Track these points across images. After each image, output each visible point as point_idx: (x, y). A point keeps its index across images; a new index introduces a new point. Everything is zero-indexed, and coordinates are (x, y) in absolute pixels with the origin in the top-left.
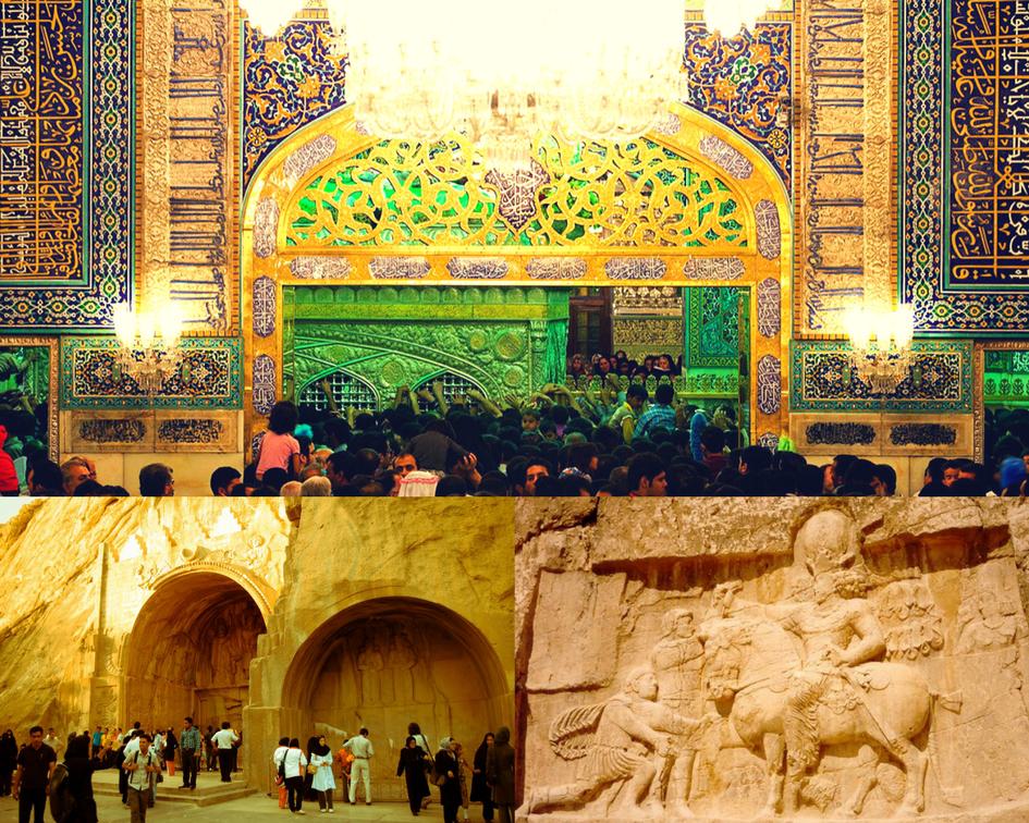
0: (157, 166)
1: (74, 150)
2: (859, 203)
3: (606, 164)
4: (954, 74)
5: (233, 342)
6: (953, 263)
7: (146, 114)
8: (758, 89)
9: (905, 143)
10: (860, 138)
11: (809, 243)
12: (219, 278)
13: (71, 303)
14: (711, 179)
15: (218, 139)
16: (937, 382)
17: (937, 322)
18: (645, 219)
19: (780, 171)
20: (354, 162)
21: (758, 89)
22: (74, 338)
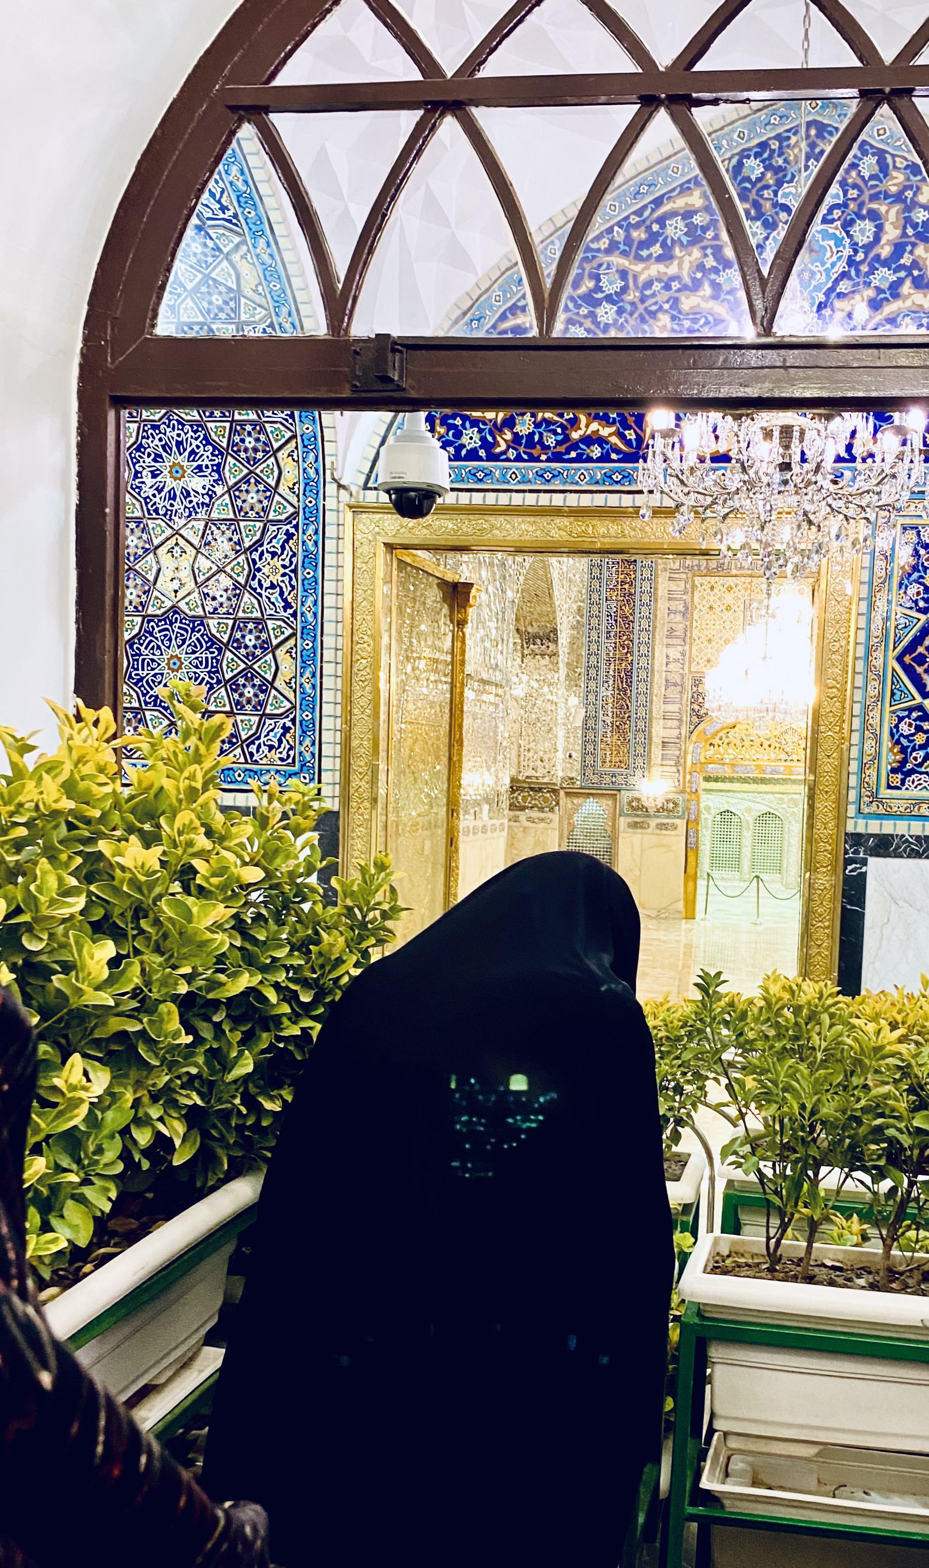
15: (680, 720)
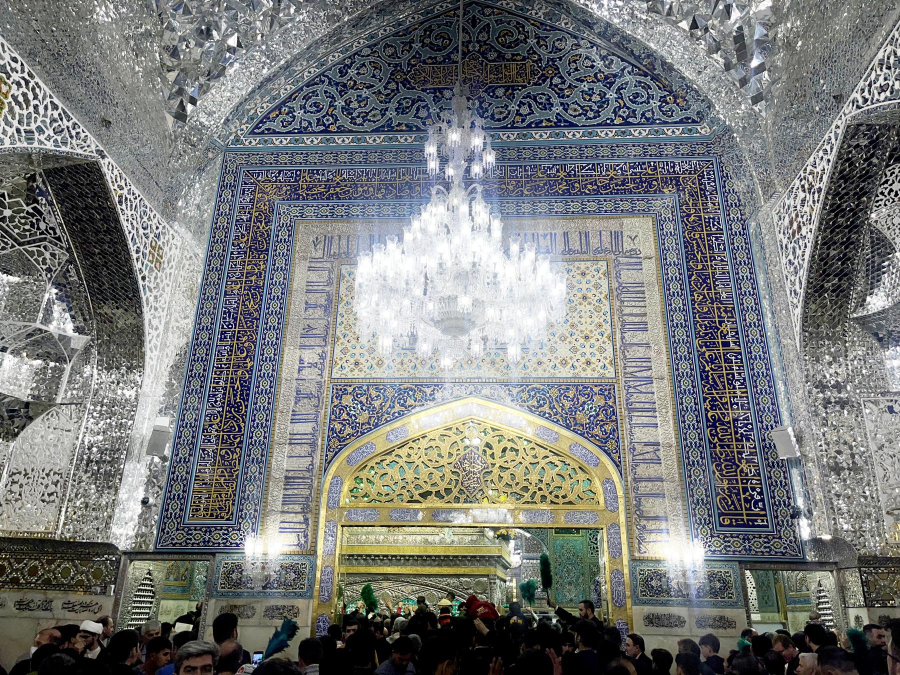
0: (280, 459)
1: (238, 450)
2: (662, 480)
3: (519, 459)
4: (706, 409)
5: (311, 558)
6: (720, 515)
7: (277, 431)
8: (600, 418)
9: (684, 447)
10: (658, 444)
11: (635, 502)
12: (306, 520)
13: (224, 534)
14: (576, 467)
15: (313, 445)
16: (720, 589)
17: (715, 551)
18: (540, 489)
19: (615, 462)
20: (383, 458)
21: (600, 418)
22: (224, 555)
